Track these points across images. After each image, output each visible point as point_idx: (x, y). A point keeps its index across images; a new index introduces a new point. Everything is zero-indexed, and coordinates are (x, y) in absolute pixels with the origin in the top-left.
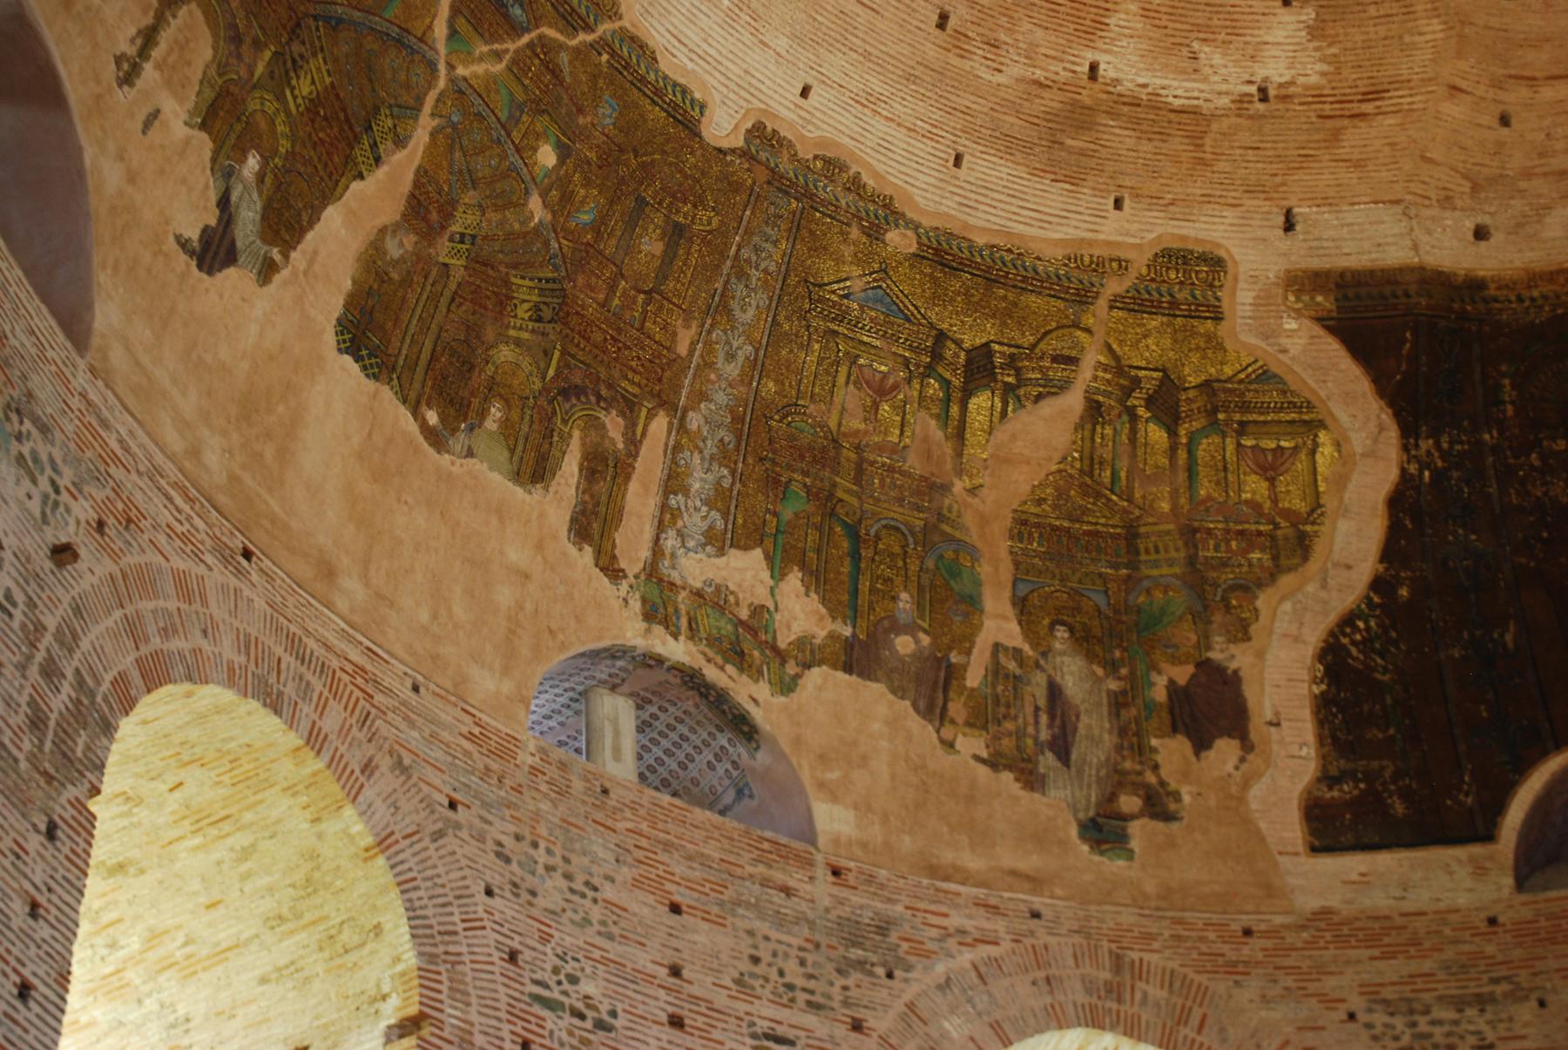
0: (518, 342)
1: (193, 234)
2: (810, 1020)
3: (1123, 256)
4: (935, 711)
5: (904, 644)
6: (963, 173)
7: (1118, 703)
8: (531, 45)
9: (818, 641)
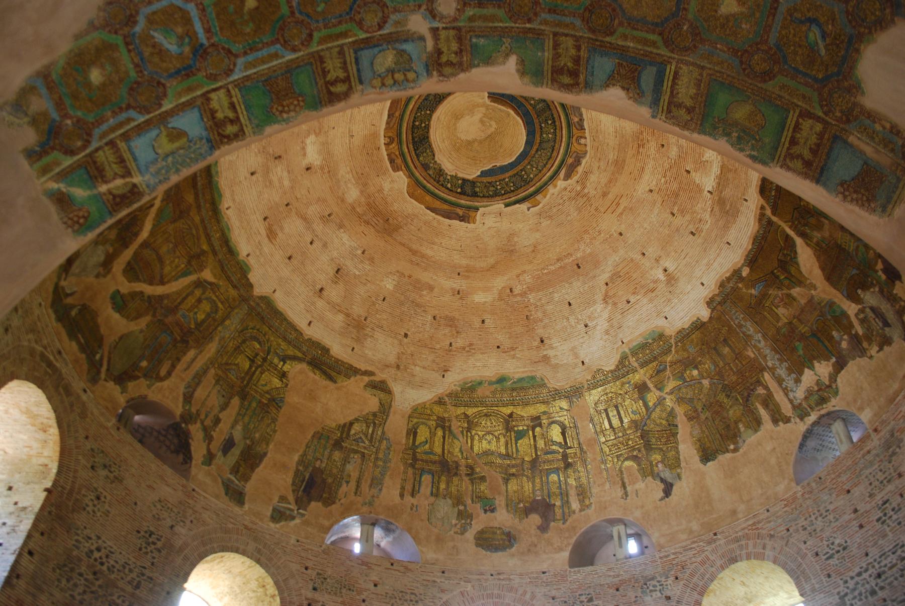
0: (731, 407)
1: (662, 494)
2: (890, 487)
3: (760, 206)
4: (863, 353)
5: (844, 345)
6: (732, 244)
7: (881, 291)
8: (670, 366)
9: (832, 371)
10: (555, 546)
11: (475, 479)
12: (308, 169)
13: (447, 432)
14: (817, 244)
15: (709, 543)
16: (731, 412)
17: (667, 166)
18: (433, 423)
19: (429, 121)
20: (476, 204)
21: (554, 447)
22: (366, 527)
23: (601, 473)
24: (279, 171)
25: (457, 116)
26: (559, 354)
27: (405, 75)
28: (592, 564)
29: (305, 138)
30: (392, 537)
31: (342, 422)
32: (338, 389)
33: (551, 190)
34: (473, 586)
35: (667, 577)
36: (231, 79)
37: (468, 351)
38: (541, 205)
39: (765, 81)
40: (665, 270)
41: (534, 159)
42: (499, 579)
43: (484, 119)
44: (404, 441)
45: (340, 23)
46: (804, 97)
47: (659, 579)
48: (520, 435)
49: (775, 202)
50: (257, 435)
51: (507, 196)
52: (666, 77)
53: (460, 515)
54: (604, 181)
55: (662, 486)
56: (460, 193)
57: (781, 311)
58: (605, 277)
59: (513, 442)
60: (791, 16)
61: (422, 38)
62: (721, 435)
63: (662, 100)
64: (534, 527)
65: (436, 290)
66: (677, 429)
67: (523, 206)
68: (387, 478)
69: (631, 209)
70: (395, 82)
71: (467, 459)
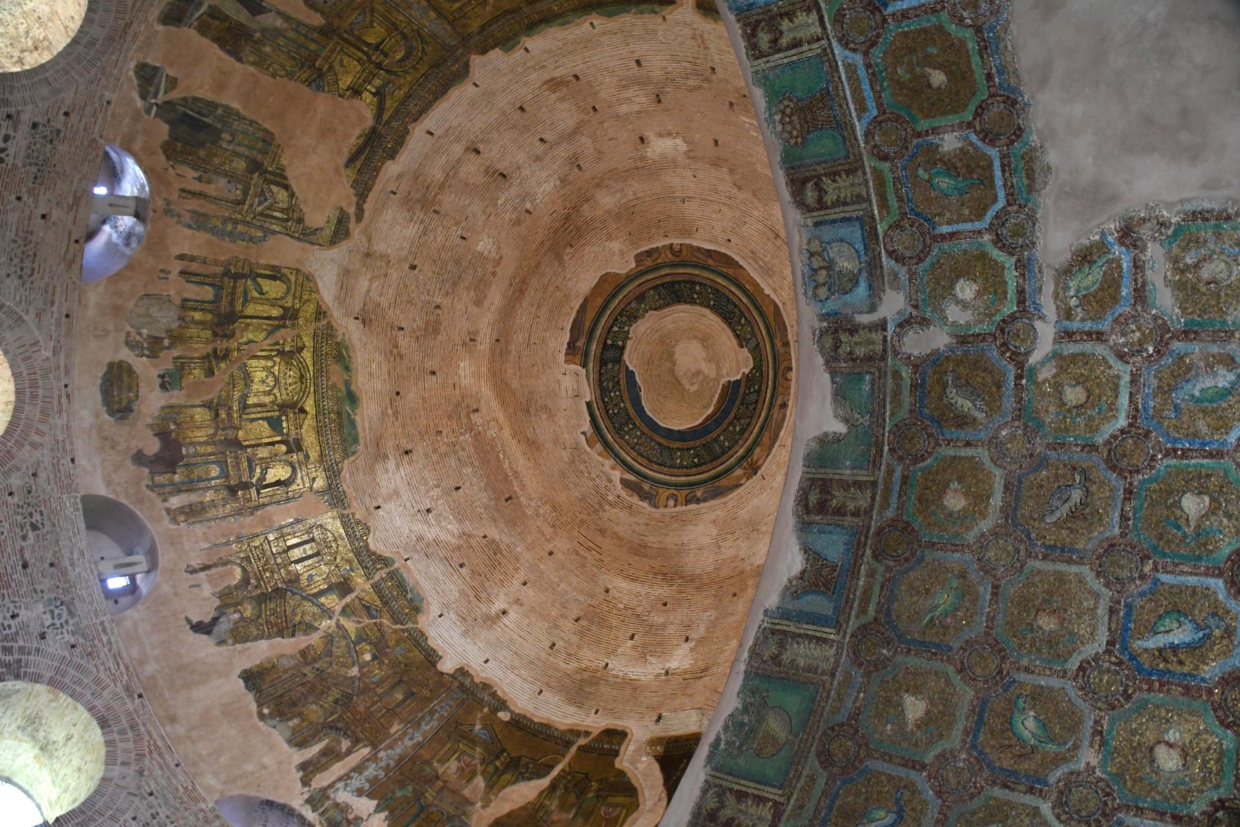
0: (321, 706)
1: (195, 620)
3: (589, 730)
6: (540, 697)
8: (375, 623)
10: (113, 476)
11: (210, 362)
12: (642, 139)
13: (277, 322)
14: (542, 806)
15: (127, 689)
16: (314, 707)
17: (639, 610)
18: (289, 302)
19: (701, 304)
20: (591, 365)
21: (258, 470)
22: (133, 205)
23: (223, 536)
24: (640, 99)
25: (705, 340)
26: (390, 475)
27: (824, 285)
28: (89, 527)
29: (684, 137)
30: (119, 241)
31: (288, 173)
32: (337, 170)
33: (609, 463)
34: (48, 359)
35: (73, 633)
36: (835, 43)
37: (391, 352)
38: (588, 449)
39: (818, 756)
40: (504, 613)
41: (649, 440)
42: (60, 397)
43: (701, 377)
44: (262, 261)
45: (900, 199)
46: (801, 807)
47: (71, 622)
48: (275, 424)
49: (594, 749)
50: (268, 49)
51: (601, 404)
52: (819, 628)
53: (155, 341)
54: (620, 530)
55: (207, 620)
56: (605, 343)
57: (453, 765)
58: (494, 533)
59: (265, 415)
60: (905, 787)
61: (873, 308)
62: (281, 696)
63: (788, 623)
64: (141, 445)
65: (475, 310)
66: (288, 637)
67: (587, 427)
68: (207, 236)
69: (584, 566)
70: (815, 271)
71: (239, 350)
